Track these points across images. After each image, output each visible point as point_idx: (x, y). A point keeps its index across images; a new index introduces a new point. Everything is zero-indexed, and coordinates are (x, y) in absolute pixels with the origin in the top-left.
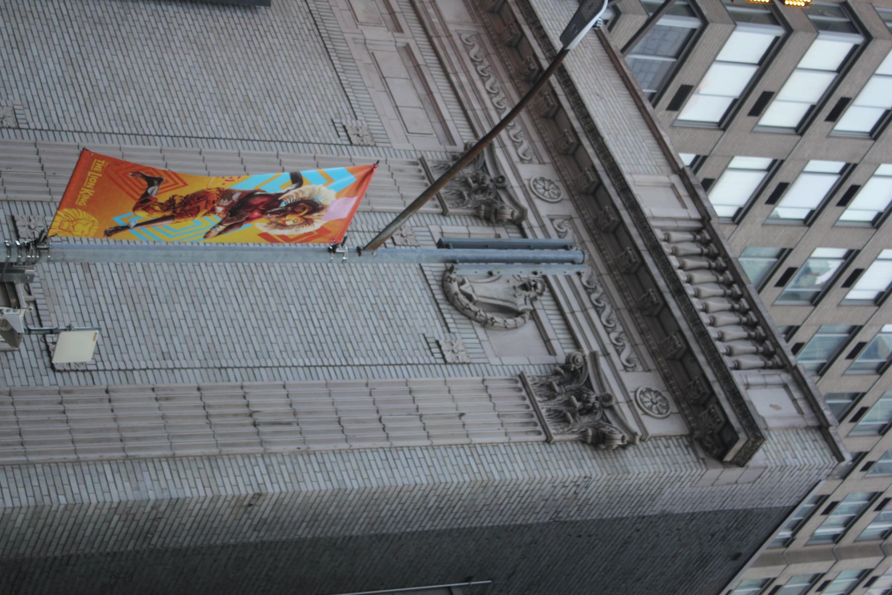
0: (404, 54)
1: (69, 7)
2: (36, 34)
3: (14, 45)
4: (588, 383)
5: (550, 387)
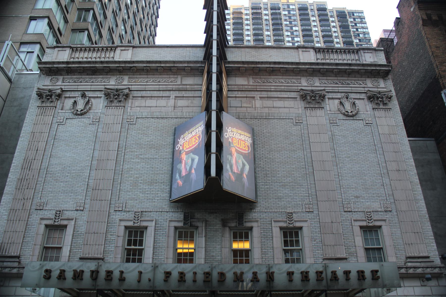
0: (262, 99)
4: (375, 95)
5: (377, 103)
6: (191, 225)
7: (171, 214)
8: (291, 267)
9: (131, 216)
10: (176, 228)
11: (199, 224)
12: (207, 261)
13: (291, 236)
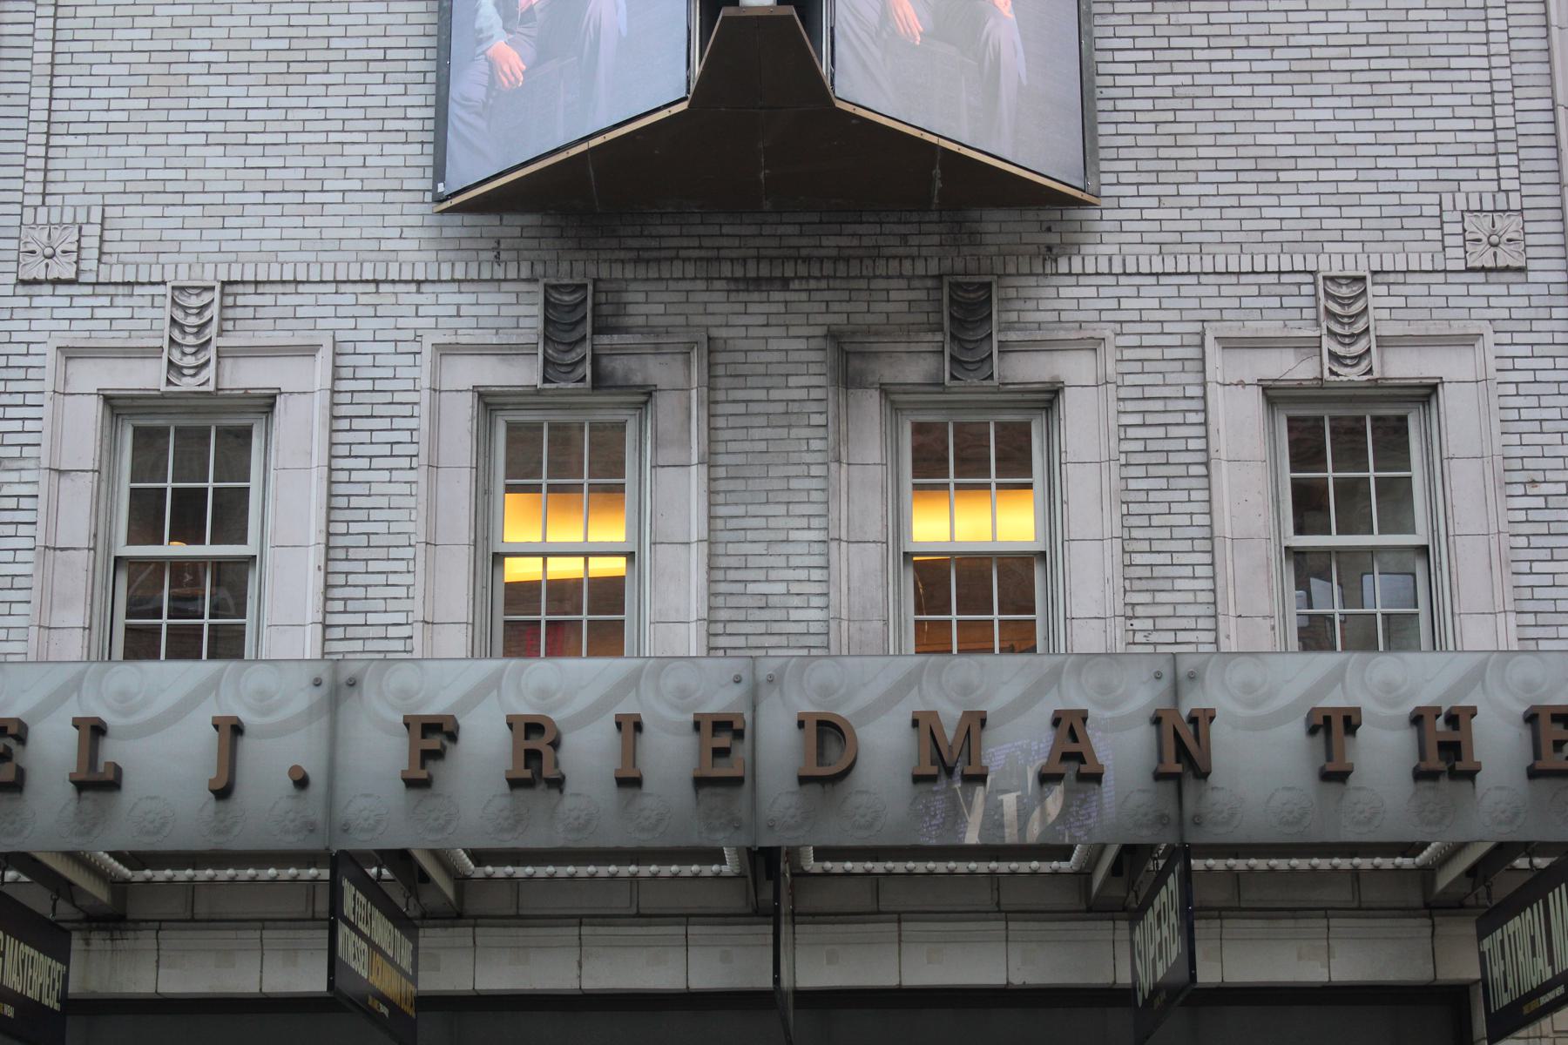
1: (1128, 43)
2: (1229, 128)
3: (1272, 176)
6: (600, 381)
7: (450, 297)
8: (1338, 676)
9: (148, 319)
10: (488, 402)
11: (656, 370)
12: (722, 642)
13: (1351, 454)
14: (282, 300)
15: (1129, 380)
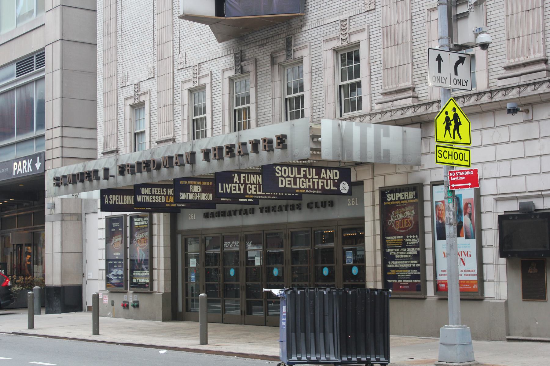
6: (242, 72)
7: (224, 59)
9: (188, 74)
14: (206, 65)
15: (313, 53)
